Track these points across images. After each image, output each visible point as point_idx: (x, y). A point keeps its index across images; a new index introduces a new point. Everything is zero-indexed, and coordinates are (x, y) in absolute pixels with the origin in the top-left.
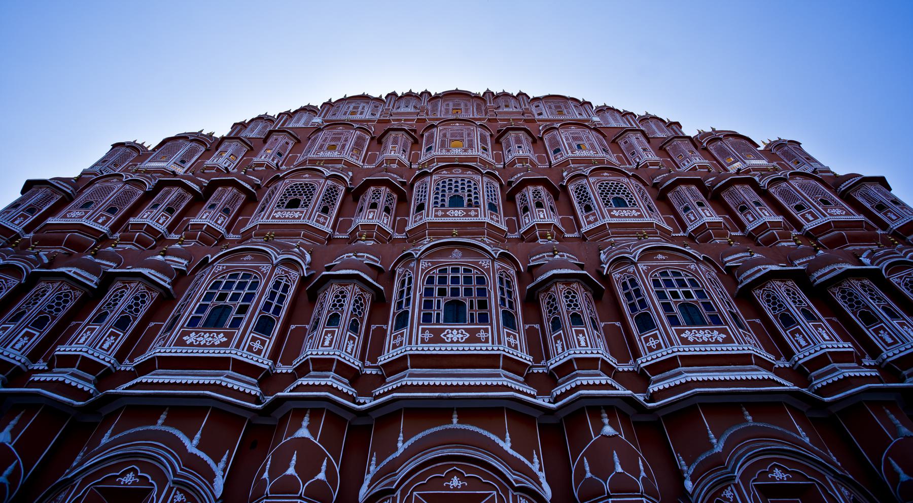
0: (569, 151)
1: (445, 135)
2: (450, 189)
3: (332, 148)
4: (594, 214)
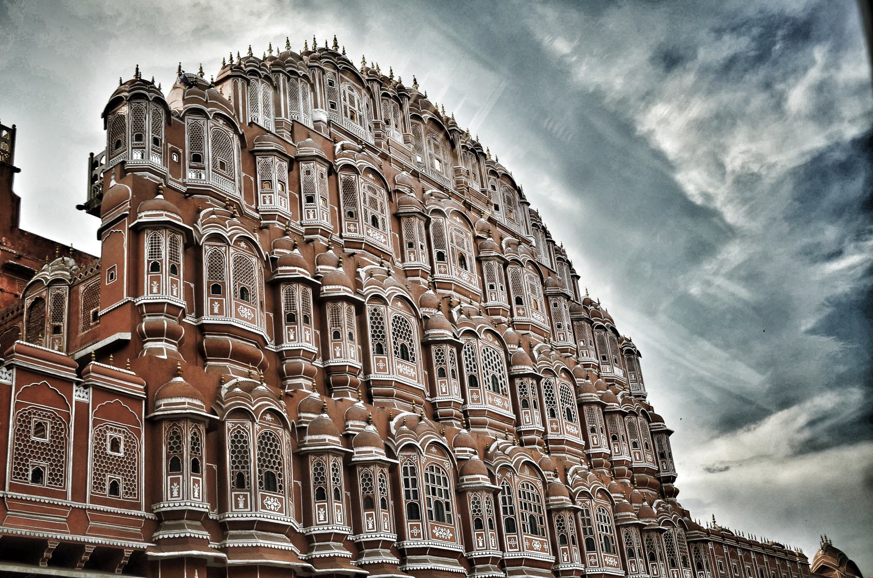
1: (452, 241)
3: (375, 221)
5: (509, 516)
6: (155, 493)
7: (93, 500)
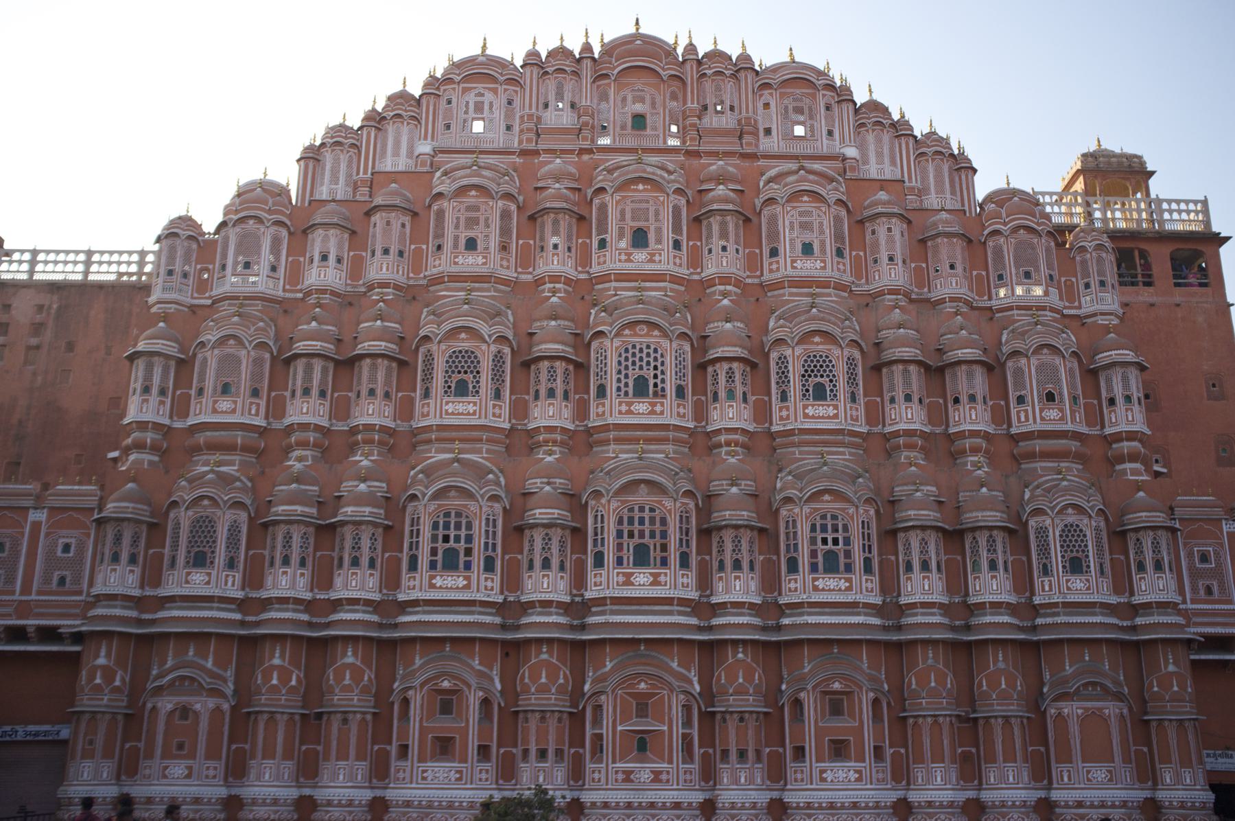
0: (789, 260)
1: (623, 218)
2: (634, 363)
3: (471, 244)
4: (788, 408)
5: (599, 548)
6: (91, 584)
7: (39, 593)
